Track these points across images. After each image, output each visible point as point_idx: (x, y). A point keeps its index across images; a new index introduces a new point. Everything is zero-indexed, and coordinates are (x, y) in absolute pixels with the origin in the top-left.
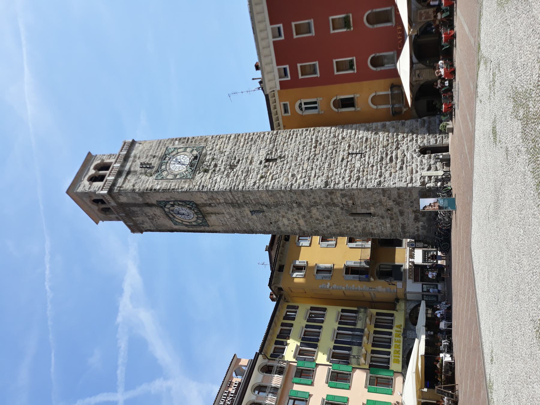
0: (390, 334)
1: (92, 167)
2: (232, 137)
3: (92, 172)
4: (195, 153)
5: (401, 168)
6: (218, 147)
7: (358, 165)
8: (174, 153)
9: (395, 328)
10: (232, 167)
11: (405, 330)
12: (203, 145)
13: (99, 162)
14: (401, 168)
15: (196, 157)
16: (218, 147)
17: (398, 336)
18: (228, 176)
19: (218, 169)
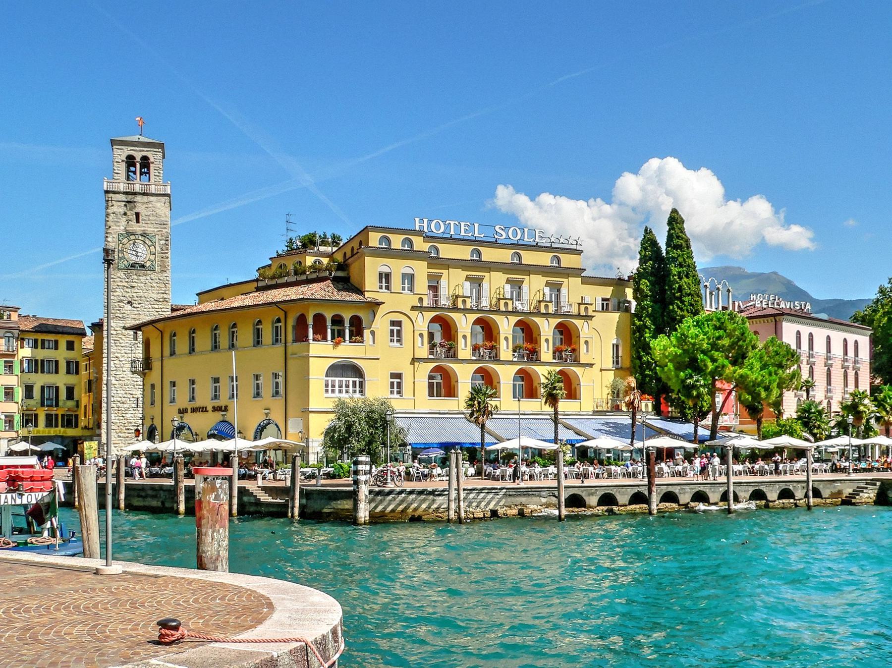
0: (57, 426)
1: (144, 154)
2: (165, 296)
3: (138, 156)
4: (148, 264)
5: (119, 436)
6: (155, 285)
7: (125, 406)
8: (150, 243)
9: (63, 429)
10: (129, 302)
11: (62, 437)
12: (157, 269)
13: (152, 160)
14: (119, 436)
15: (143, 266)
16: (155, 285)
17: (55, 431)
18: (121, 301)
19: (129, 290)
